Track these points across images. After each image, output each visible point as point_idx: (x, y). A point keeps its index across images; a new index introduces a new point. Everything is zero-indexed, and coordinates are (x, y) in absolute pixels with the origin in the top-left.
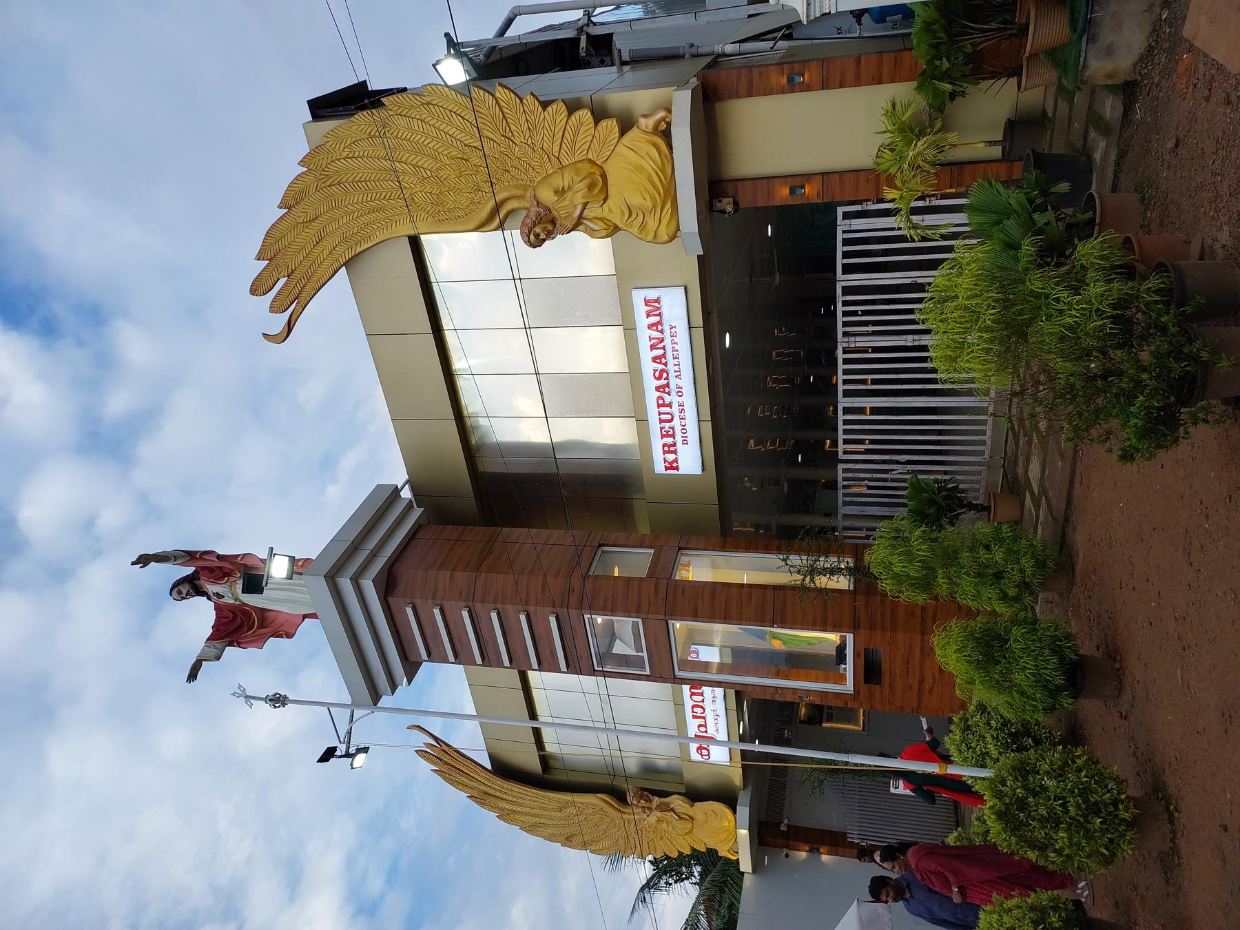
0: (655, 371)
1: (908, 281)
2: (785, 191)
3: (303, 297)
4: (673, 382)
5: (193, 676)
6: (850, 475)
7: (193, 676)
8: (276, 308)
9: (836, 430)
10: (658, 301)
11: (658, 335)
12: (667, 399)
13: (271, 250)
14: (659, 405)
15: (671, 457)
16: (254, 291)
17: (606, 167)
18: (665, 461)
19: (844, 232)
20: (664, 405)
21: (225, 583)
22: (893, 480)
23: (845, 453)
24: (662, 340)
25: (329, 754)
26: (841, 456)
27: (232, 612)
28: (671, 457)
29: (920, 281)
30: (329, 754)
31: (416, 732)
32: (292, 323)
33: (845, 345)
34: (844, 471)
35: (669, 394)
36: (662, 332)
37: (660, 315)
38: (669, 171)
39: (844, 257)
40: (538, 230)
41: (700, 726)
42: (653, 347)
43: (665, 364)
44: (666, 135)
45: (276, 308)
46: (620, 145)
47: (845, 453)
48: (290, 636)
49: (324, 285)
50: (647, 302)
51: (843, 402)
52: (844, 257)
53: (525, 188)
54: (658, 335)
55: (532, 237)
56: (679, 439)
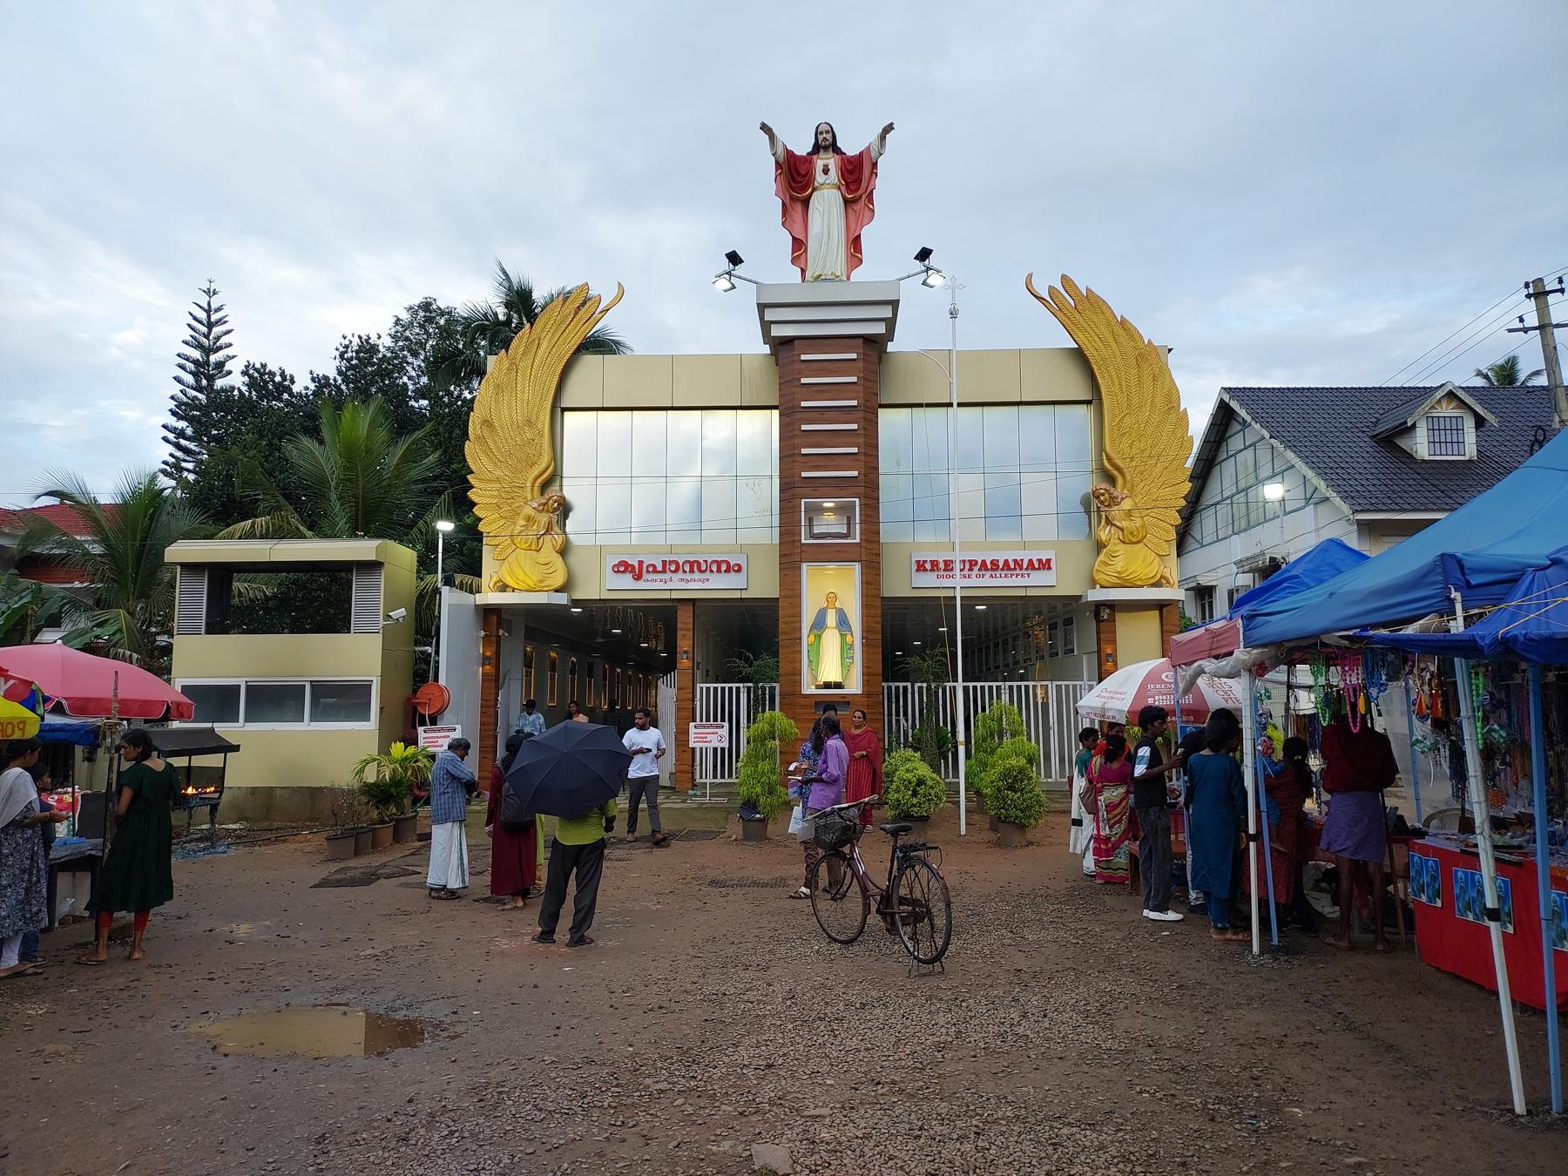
0: (998, 561)
1: (1051, 724)
2: (1109, 651)
3: (1059, 314)
4: (988, 574)
5: (765, 128)
6: (893, 692)
7: (765, 128)
8: (1051, 290)
9: (724, 682)
10: (1049, 568)
11: (1025, 567)
12: (976, 568)
13: (1091, 302)
14: (970, 561)
15: (928, 566)
16: (1065, 280)
17: (1141, 544)
18: (925, 562)
19: (1081, 685)
20: (971, 565)
21: (839, 180)
22: (898, 721)
23: (701, 688)
24: (1021, 569)
25: (734, 258)
26: (917, 685)
27: (807, 173)
28: (928, 566)
29: (1052, 732)
30: (734, 258)
31: (615, 291)
32: (1046, 303)
33: (1003, 687)
34: (905, 688)
35: (980, 570)
36: (1027, 569)
37: (1039, 569)
38: (1139, 583)
39: (997, 686)
40: (1107, 495)
41: (654, 566)
42: (1015, 561)
43: (1003, 569)
44: (1157, 585)
45: (1051, 290)
46: (1155, 555)
47: (701, 688)
48: (783, 224)
49: (1071, 335)
50: (1049, 561)
51: (1005, 685)
52: (997, 686)
53: (1131, 491)
54: (1025, 567)
55: (1103, 491)
56: (942, 573)
